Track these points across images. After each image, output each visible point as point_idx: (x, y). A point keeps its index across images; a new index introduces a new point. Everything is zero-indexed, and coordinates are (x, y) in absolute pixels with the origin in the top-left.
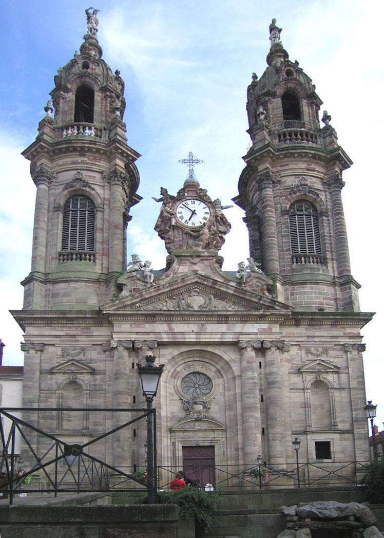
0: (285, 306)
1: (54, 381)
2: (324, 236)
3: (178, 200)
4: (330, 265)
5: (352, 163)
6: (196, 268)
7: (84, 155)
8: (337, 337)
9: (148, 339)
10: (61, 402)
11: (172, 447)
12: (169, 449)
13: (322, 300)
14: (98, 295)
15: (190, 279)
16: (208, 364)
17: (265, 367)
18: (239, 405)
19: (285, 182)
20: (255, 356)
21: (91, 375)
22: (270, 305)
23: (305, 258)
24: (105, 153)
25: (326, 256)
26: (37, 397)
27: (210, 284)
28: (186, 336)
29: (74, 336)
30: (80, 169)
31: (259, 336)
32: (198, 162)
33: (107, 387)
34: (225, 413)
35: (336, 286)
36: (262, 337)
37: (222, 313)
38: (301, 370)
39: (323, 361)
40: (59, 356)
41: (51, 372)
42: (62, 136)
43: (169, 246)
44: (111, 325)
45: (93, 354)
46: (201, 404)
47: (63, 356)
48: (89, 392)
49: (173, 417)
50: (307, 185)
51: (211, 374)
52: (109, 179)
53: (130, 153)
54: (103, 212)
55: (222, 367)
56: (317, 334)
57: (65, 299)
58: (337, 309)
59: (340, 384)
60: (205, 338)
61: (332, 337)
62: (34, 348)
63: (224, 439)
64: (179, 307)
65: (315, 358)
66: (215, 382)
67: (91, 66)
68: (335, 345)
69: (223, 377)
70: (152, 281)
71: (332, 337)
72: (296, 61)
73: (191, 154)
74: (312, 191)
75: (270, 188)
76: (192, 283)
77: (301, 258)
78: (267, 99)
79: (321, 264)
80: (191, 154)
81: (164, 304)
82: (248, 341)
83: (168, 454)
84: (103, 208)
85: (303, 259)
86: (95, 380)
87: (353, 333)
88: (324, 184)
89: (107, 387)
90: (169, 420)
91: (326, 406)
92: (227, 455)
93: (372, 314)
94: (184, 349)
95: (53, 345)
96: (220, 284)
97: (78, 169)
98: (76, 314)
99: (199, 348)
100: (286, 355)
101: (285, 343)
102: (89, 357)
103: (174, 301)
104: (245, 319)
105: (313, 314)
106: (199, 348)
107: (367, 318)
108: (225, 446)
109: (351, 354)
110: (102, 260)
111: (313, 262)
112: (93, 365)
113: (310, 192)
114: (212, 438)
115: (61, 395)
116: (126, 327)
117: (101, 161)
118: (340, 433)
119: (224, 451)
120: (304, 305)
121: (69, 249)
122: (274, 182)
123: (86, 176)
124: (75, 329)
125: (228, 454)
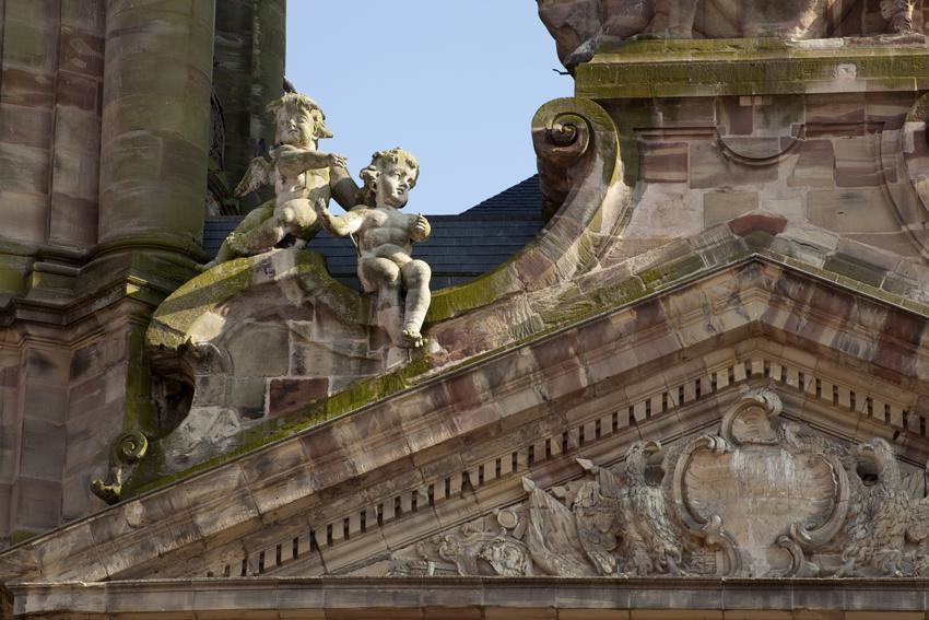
6: (767, 198)
64: (620, 544)
70: (415, 328)
76: (719, 342)
81: (509, 518)
103: (582, 492)
110: (48, 143)
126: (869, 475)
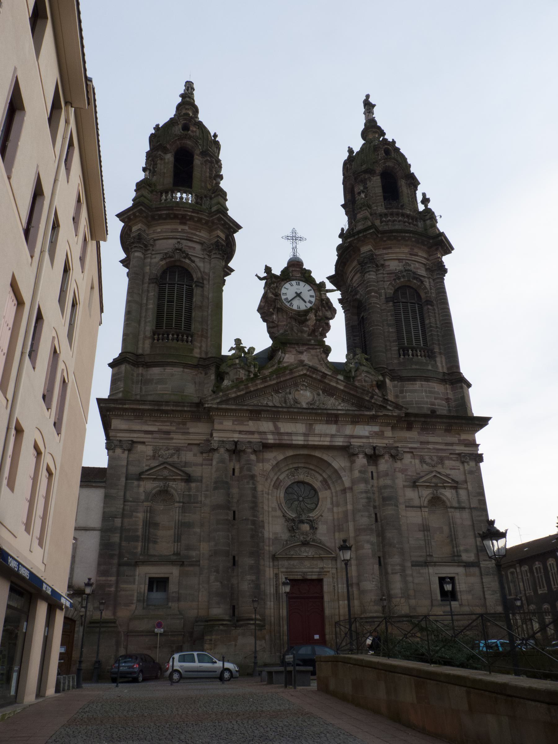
0: (397, 406)
1: (141, 490)
2: (431, 327)
3: (283, 280)
4: (438, 359)
5: (453, 249)
7: (185, 224)
8: (452, 444)
9: (252, 440)
10: (148, 517)
11: (275, 580)
12: (272, 584)
13: (433, 400)
14: (195, 383)
15: (299, 371)
16: (313, 472)
17: (378, 478)
18: (351, 525)
19: (389, 265)
20: (367, 464)
21: (185, 482)
22: (382, 404)
23: (412, 351)
24: (207, 223)
25: (434, 349)
26: (121, 510)
27: (319, 378)
28: (294, 438)
29: (168, 433)
30: (180, 239)
31: (371, 441)
32: (301, 239)
33: (203, 499)
34: (334, 535)
35: (446, 384)
36: (376, 442)
37: (333, 412)
38: (417, 484)
39: (439, 473)
40: (149, 458)
41: (139, 477)
42: (161, 200)
43: (272, 330)
44: (211, 420)
45: (189, 456)
46: (307, 523)
47: (154, 457)
48: (181, 504)
49: (276, 539)
50: (411, 271)
51: (317, 485)
52: (210, 252)
53: (231, 225)
54: (202, 287)
55: (329, 477)
56: (431, 439)
57: (159, 386)
58: (450, 411)
59: (459, 502)
60: (314, 441)
61: (447, 444)
62: (121, 447)
63: (334, 571)
64: (285, 402)
65: (431, 468)
66: (323, 494)
67: (191, 129)
68: (451, 454)
69: (330, 488)
71: (447, 444)
72: (393, 140)
73: (294, 231)
74: (417, 277)
75: (373, 271)
77: (408, 351)
78: (367, 176)
79: (425, 357)
80: (294, 231)
82: (360, 446)
83: (270, 590)
84: (203, 284)
85: (410, 352)
86: (190, 489)
87: (468, 440)
88: (427, 270)
89: (203, 499)
90: (271, 543)
91: (446, 529)
92: (338, 592)
93: (488, 419)
94: (290, 453)
95: (143, 443)
96: (330, 377)
97: (177, 238)
98: (173, 406)
99: (305, 452)
100: (398, 465)
101: (399, 449)
102: (184, 459)
103: (280, 395)
104: (356, 420)
105: (425, 416)
106: (305, 452)
107: (483, 422)
108: (335, 580)
109: (468, 465)
111: (421, 356)
112: (187, 469)
113: (415, 278)
114: (320, 568)
115: (149, 508)
116: (228, 424)
117: (202, 231)
118: (465, 566)
119: (334, 586)
120: (414, 405)
121: (164, 327)
122: (377, 266)
123: (185, 246)
124: (169, 424)
125: (340, 591)
126: (318, 395)
